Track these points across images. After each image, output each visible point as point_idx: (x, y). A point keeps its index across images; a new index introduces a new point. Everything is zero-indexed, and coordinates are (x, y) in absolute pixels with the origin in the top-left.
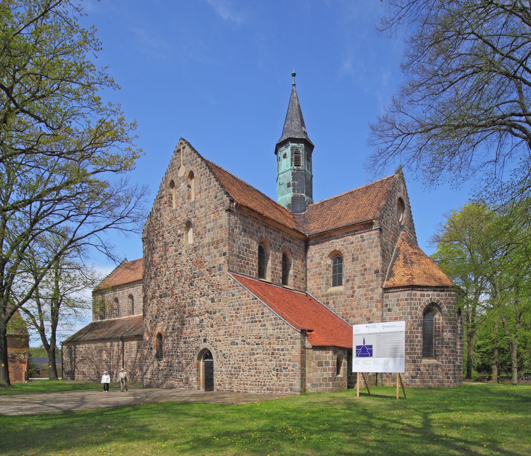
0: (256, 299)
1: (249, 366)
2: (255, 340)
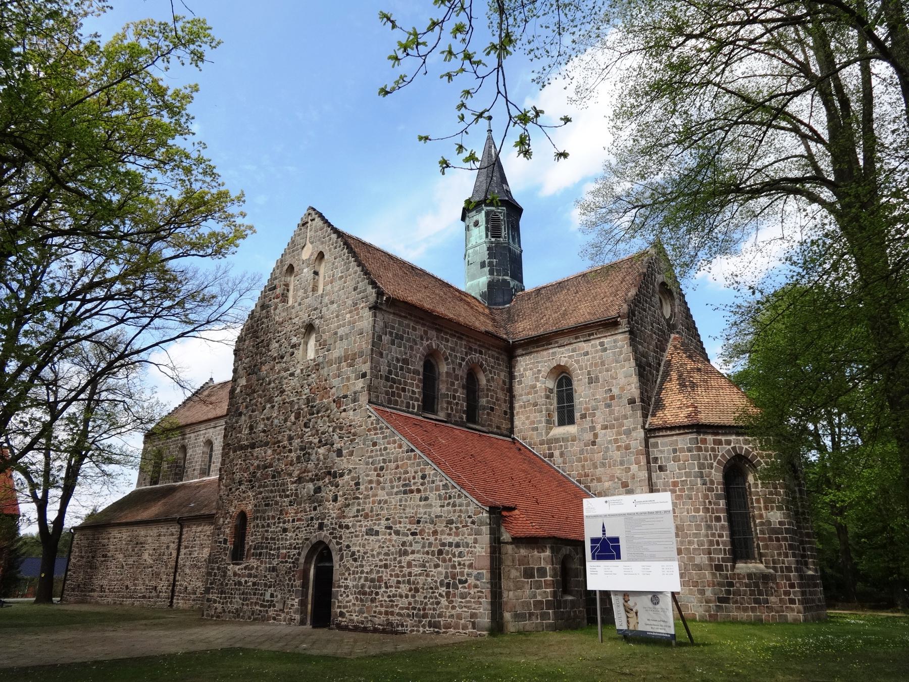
0: (412, 451)
1: (397, 576)
2: (408, 526)
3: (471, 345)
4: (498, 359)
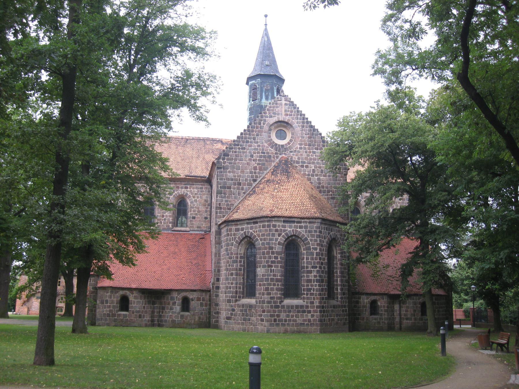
3: (178, 185)
4: (202, 188)
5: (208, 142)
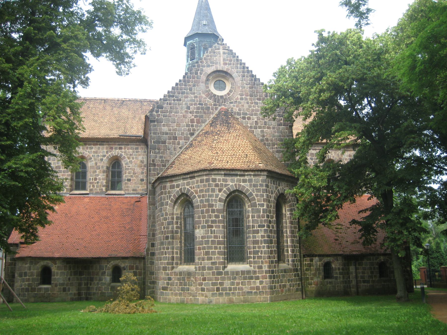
5: (145, 104)
